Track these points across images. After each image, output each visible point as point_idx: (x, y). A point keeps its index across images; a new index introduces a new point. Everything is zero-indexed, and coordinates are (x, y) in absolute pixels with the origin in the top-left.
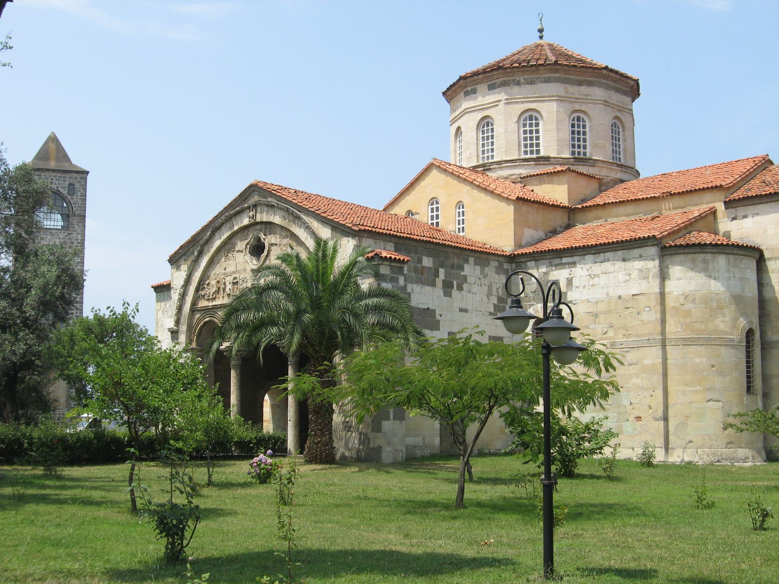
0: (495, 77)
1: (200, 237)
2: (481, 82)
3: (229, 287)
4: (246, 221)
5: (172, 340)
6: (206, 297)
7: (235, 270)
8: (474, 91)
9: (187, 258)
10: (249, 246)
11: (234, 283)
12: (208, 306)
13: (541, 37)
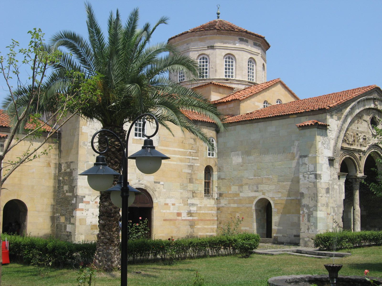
0: (258, 40)
1: (348, 103)
4: (372, 106)
5: (330, 165)
8: (247, 41)
9: (338, 112)
11: (364, 139)
12: (350, 148)
13: (218, 17)
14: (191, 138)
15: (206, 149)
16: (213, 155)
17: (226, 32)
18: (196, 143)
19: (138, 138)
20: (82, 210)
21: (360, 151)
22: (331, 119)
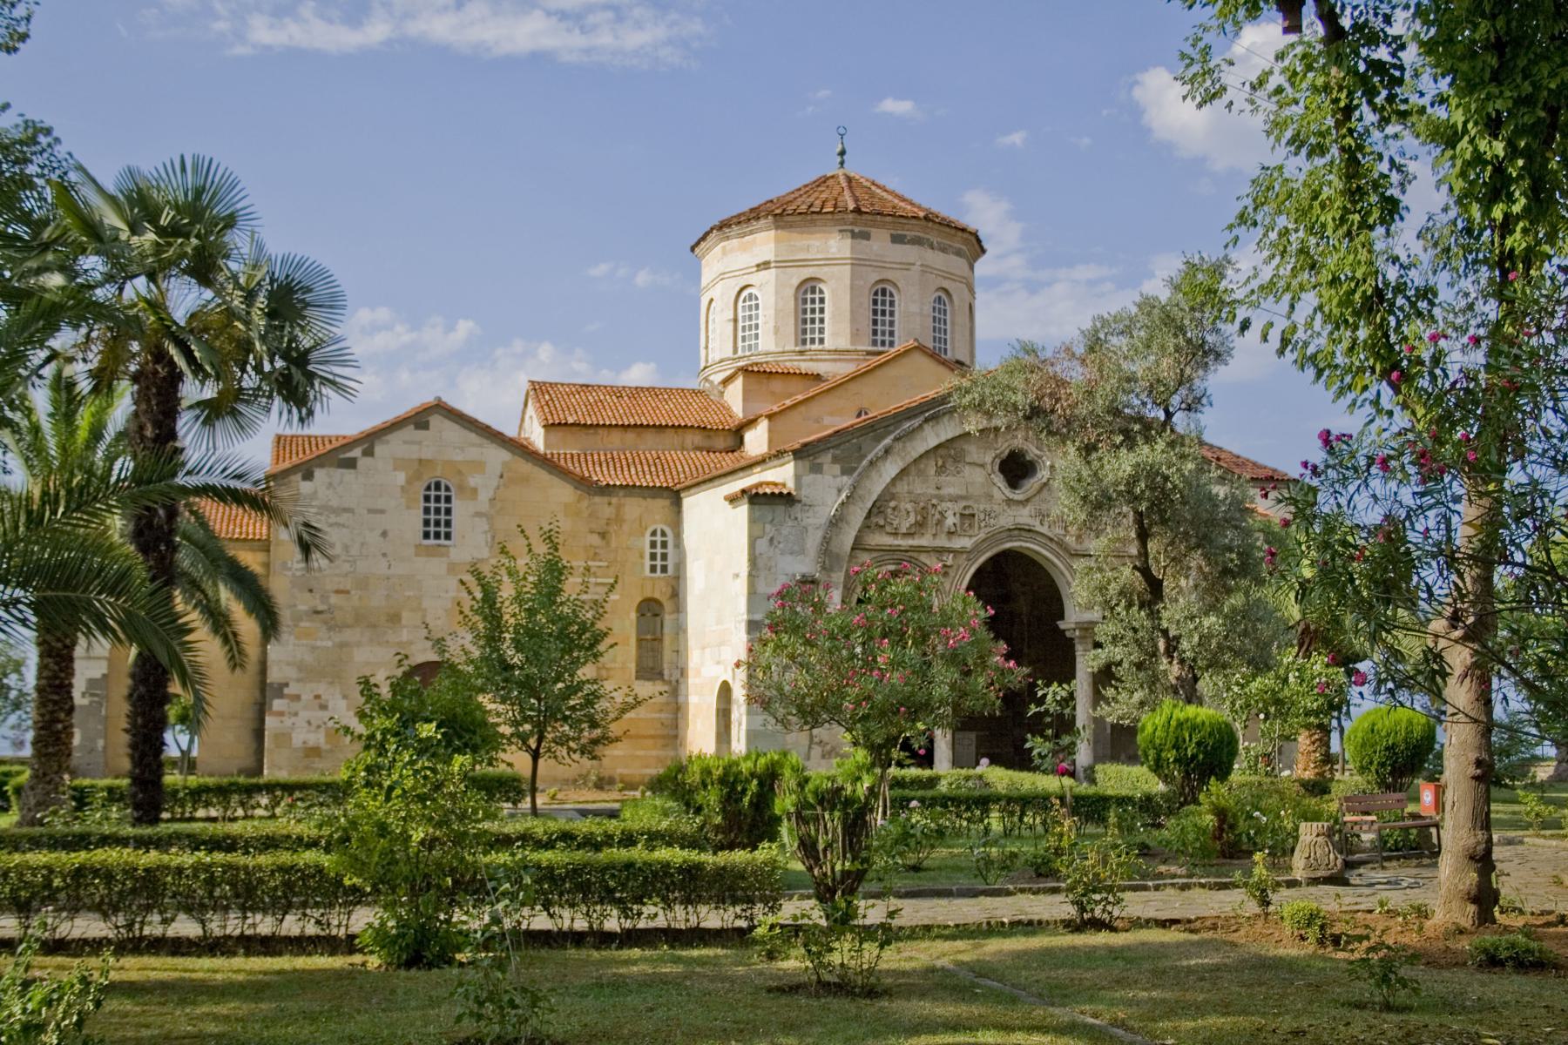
2: (883, 226)
3: (950, 520)
6: (888, 529)
7: (964, 493)
10: (998, 461)
14: (592, 532)
15: (642, 557)
16: (664, 569)
17: (799, 218)
18: (608, 544)
19: (432, 541)
20: (281, 714)
21: (940, 551)
22: (812, 476)
